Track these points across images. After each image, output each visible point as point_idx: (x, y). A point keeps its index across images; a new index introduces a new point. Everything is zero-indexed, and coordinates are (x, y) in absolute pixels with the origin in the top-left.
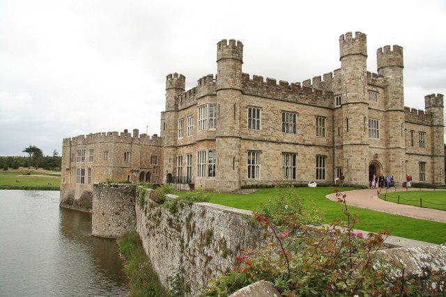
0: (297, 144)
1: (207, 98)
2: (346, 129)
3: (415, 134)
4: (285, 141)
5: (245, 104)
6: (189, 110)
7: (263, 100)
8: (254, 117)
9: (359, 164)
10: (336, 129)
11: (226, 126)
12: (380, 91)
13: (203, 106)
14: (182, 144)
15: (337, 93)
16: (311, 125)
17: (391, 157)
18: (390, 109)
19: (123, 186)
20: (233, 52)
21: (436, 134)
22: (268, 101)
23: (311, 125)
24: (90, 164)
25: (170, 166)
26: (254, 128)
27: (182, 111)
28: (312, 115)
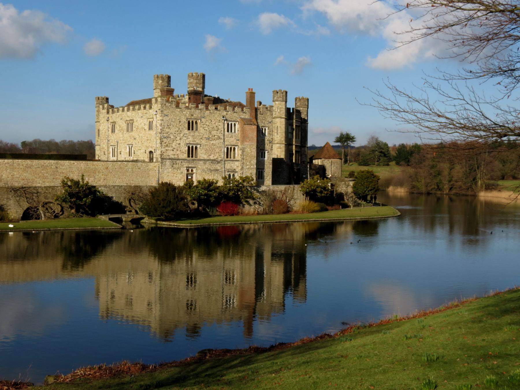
20: (97, 103)
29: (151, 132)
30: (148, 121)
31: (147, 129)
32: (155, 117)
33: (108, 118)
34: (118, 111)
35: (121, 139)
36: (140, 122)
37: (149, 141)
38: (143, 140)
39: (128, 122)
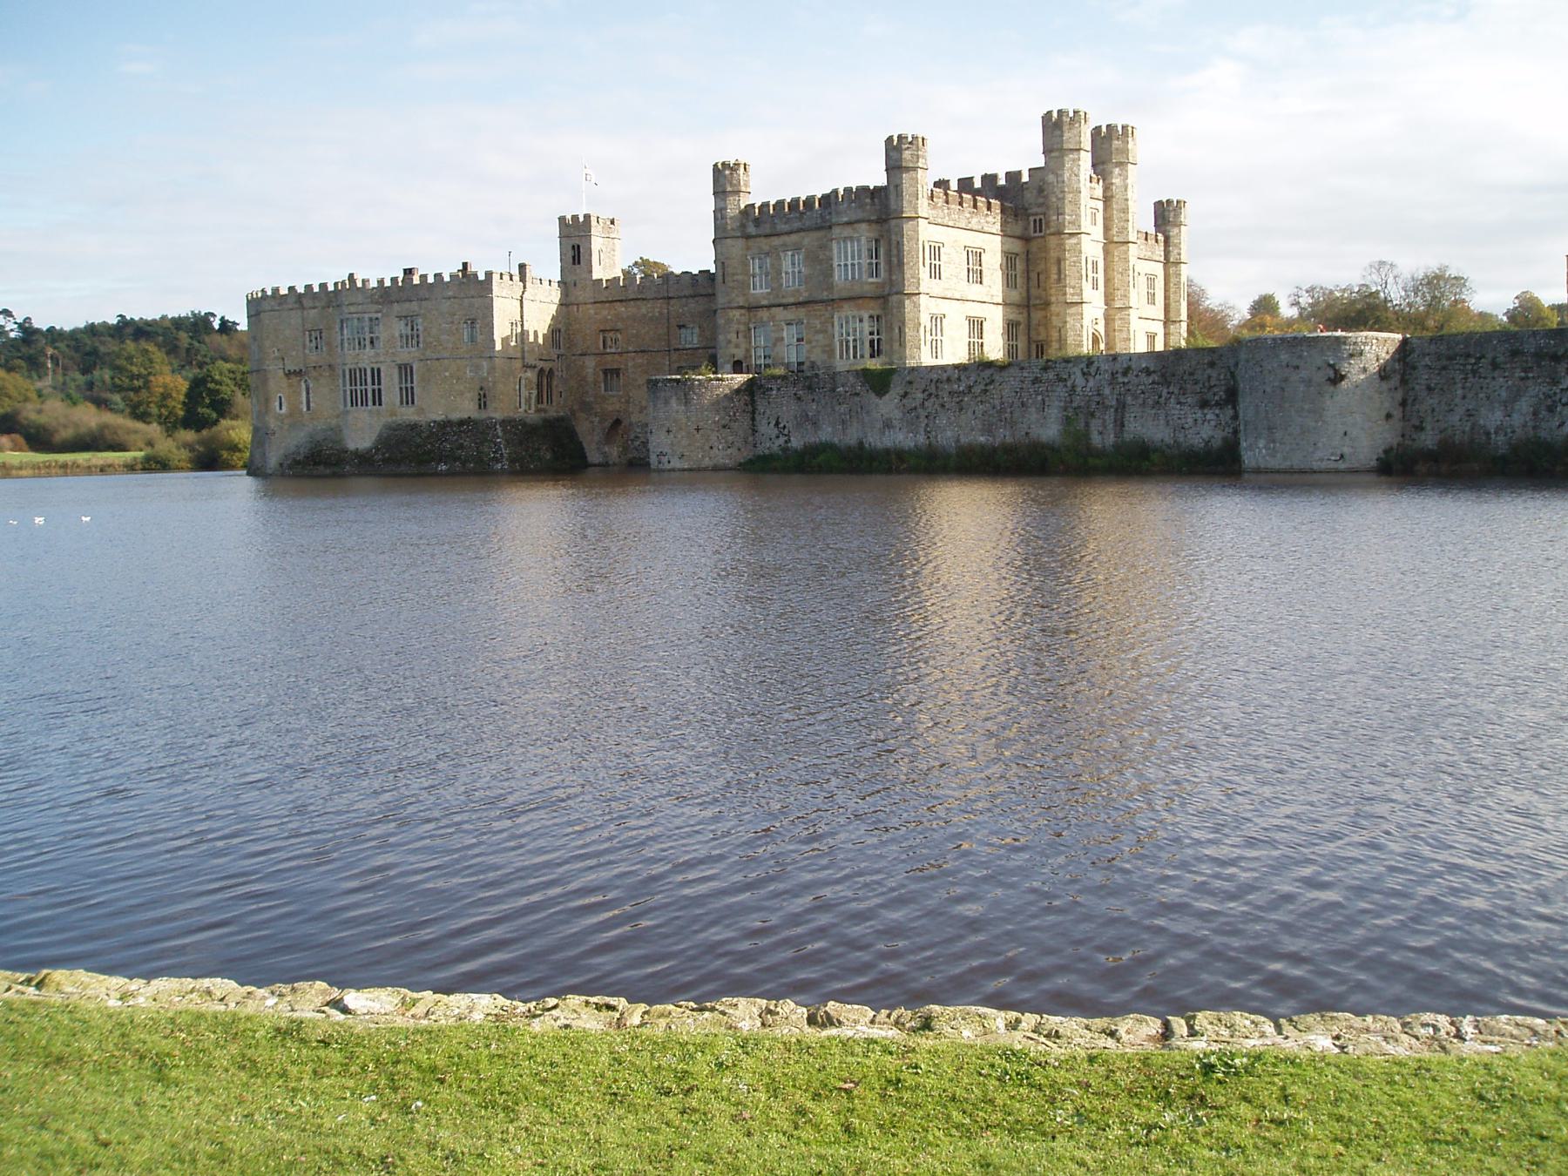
1: (864, 226)
2: (1056, 277)
6: (786, 238)
9: (1079, 335)
10: (1034, 276)
11: (913, 278)
13: (851, 239)
14: (765, 302)
15: (1035, 210)
17: (1117, 324)
18: (1116, 239)
19: (732, 379)
21: (1173, 280)
24: (405, 355)
25: (737, 346)
27: (762, 239)
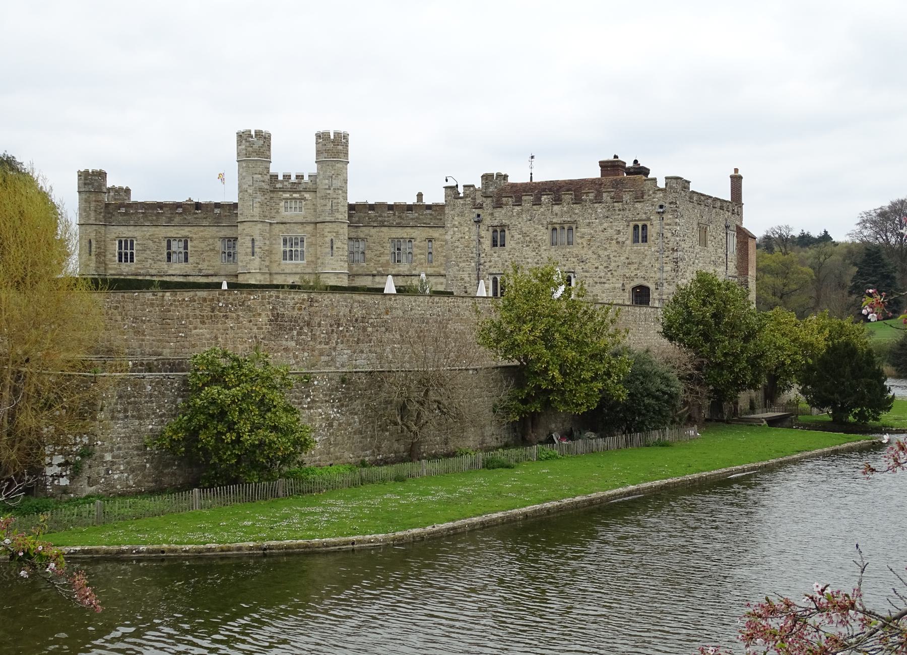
0: (189, 275)
3: (436, 244)
4: (170, 272)
5: (113, 236)
7: (138, 227)
8: (126, 248)
12: (307, 195)
16: (212, 250)
18: (318, 220)
20: (85, 184)
22: (145, 228)
23: (212, 250)
26: (126, 261)
28: (214, 238)
29: (641, 247)
30: (631, 229)
31: (629, 242)
32: (655, 219)
33: (479, 216)
34: (518, 202)
35: (529, 260)
36: (601, 228)
37: (633, 267)
38: (613, 264)
39: (557, 226)
